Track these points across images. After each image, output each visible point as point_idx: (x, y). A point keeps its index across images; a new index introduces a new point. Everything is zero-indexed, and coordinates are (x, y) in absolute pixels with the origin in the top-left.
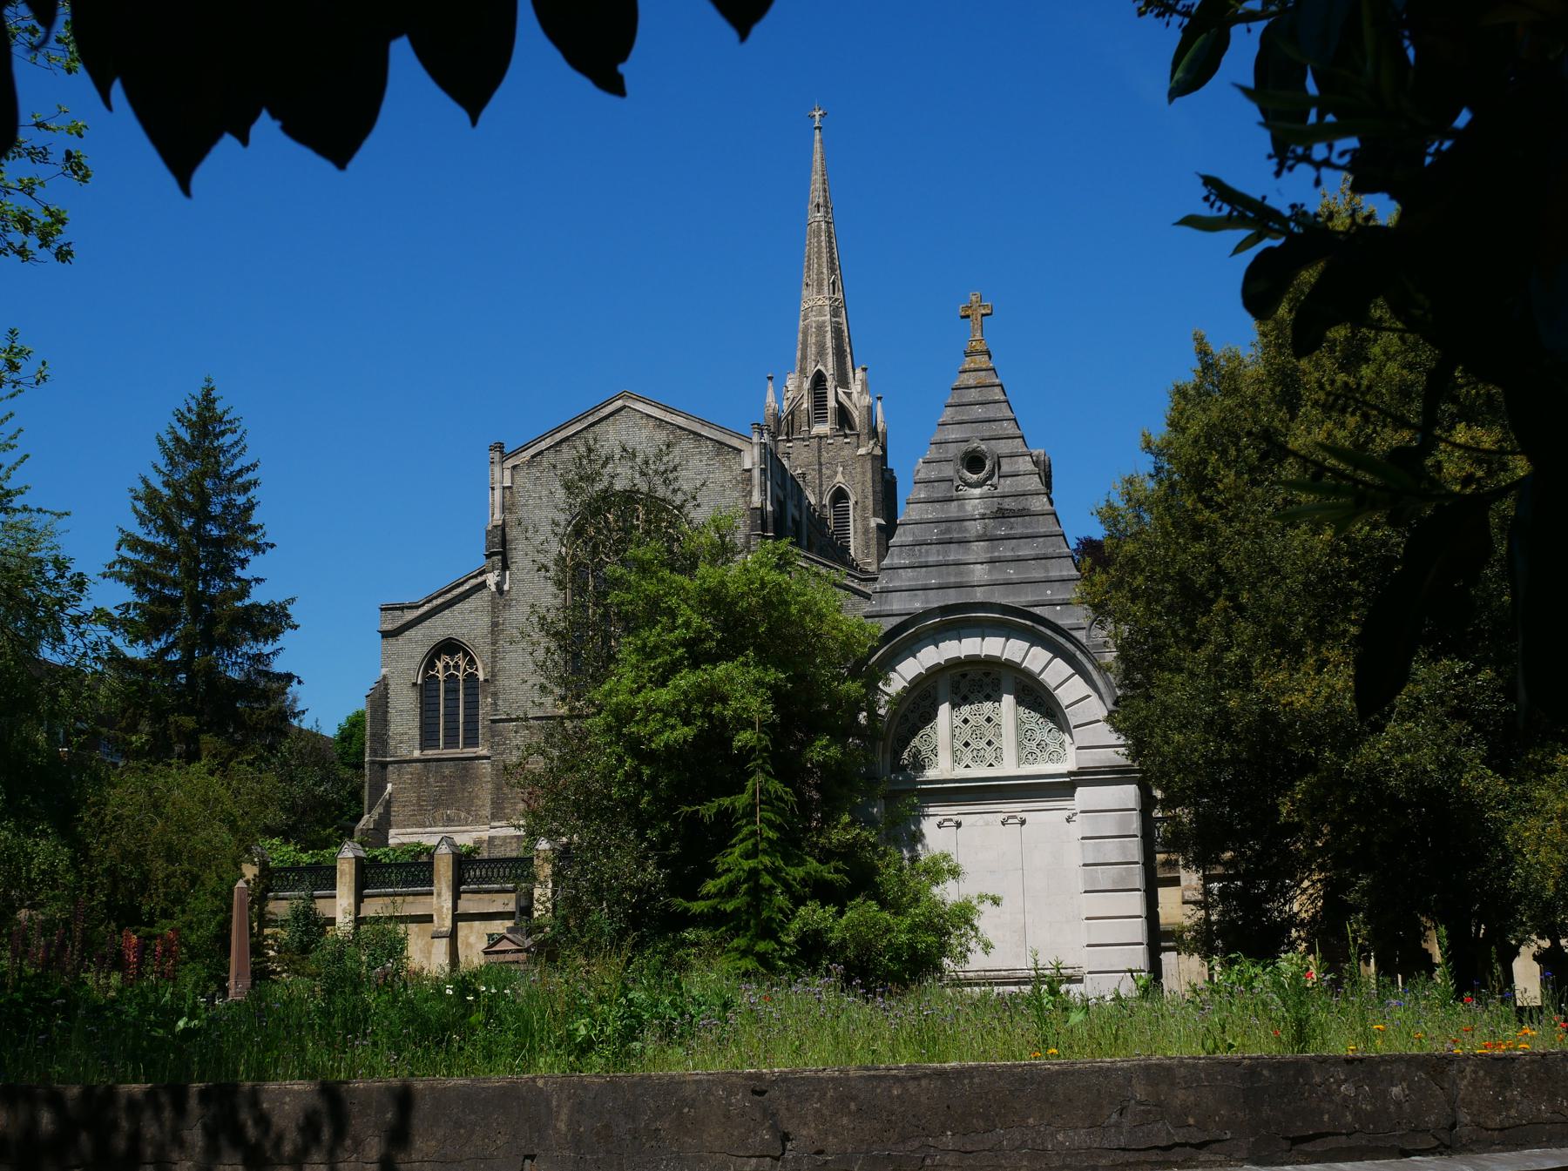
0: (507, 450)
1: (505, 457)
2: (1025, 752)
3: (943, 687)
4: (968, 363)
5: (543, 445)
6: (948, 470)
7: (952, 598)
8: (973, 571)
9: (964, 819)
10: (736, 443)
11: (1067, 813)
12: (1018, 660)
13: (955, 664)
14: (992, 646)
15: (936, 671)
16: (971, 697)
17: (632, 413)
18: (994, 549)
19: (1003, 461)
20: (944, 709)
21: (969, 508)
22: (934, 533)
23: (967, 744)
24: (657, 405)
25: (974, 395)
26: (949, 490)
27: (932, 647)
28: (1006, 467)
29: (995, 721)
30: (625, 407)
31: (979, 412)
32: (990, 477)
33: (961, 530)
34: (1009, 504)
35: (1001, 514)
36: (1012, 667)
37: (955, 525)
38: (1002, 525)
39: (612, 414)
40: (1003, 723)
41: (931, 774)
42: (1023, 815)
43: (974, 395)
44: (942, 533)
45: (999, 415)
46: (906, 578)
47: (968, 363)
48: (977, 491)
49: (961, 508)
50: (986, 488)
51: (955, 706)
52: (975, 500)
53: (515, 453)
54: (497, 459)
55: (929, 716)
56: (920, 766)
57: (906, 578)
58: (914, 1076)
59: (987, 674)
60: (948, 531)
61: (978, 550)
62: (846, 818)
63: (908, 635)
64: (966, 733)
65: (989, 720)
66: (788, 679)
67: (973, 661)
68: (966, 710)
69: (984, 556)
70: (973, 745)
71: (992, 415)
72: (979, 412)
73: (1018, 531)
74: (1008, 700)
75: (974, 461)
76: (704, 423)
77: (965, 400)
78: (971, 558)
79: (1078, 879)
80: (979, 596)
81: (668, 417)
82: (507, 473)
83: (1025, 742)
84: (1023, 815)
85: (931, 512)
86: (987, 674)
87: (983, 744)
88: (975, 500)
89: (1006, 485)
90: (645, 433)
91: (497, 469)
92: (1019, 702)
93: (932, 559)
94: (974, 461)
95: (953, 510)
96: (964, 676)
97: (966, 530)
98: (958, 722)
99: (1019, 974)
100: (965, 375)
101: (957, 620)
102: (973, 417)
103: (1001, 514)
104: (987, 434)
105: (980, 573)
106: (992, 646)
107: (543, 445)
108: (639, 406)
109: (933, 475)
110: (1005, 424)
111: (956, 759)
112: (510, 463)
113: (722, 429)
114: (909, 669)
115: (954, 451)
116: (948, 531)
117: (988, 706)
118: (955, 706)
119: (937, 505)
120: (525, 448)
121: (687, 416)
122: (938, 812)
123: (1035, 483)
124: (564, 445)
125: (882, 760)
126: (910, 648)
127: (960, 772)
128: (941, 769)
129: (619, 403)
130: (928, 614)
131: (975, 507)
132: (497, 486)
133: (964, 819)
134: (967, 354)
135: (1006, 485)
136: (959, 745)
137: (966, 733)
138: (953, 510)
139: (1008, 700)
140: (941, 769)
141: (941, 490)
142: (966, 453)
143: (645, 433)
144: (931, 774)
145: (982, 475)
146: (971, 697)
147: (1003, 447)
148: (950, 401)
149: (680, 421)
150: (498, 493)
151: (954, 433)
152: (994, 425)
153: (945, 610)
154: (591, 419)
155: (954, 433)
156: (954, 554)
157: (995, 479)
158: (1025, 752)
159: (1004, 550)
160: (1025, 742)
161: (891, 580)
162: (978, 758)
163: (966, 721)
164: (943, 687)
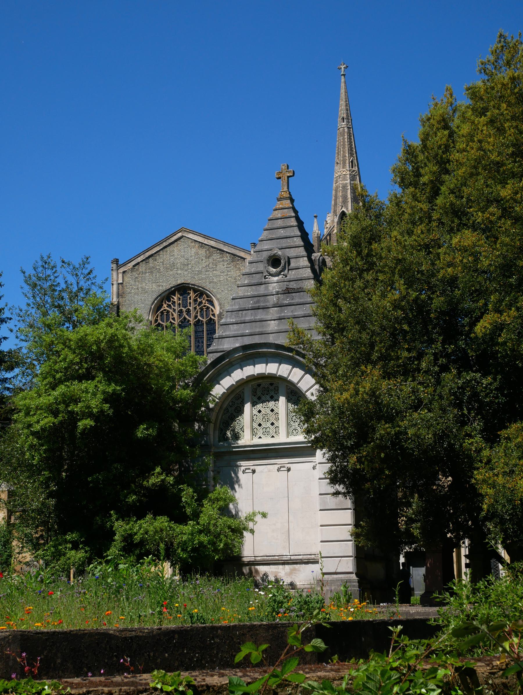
0: (120, 263)
1: (119, 267)
2: (292, 429)
3: (248, 392)
4: (279, 205)
5: (139, 259)
6: (261, 267)
7: (257, 340)
8: (269, 325)
9: (257, 468)
10: (242, 254)
11: (313, 464)
12: (285, 375)
13: (252, 379)
14: (272, 368)
15: (242, 384)
16: (263, 398)
17: (187, 240)
18: (282, 311)
19: (292, 261)
20: (247, 407)
21: (271, 288)
22: (250, 303)
23: (260, 425)
24: (200, 235)
25: (280, 223)
26: (261, 279)
27: (239, 370)
28: (293, 265)
29: (276, 411)
30: (182, 237)
31: (282, 232)
32: (283, 270)
33: (265, 301)
34: (293, 285)
35: (288, 291)
36: (282, 379)
37: (262, 299)
38: (287, 297)
39: (176, 241)
40: (280, 412)
41: (241, 442)
42: (289, 465)
43: (280, 223)
44: (255, 303)
45: (292, 234)
46: (233, 330)
47: (279, 205)
48: (276, 279)
49: (267, 288)
50: (281, 276)
51: (254, 404)
52: (275, 284)
53: (125, 264)
54: (115, 268)
55: (240, 411)
56: (236, 437)
57: (233, 330)
58: (18, 631)
59: (271, 384)
60: (258, 302)
61: (274, 312)
62: (158, 470)
63: (225, 363)
64: (259, 418)
65: (272, 410)
66: (123, 390)
67: (262, 377)
68: (259, 406)
69: (276, 316)
70: (264, 425)
71: (288, 234)
72: (282, 232)
73: (297, 300)
74: (282, 399)
75: (275, 261)
76: (225, 244)
77: (275, 226)
78: (269, 317)
79: (316, 502)
80: (271, 339)
81: (206, 242)
82: (120, 275)
83: (292, 423)
84: (289, 465)
85: (250, 291)
86: (271, 384)
87: (269, 424)
88: (275, 284)
89: (292, 275)
90: (194, 250)
91: (115, 273)
92: (289, 400)
93: (248, 318)
94: (275, 261)
95: (262, 290)
96: (259, 385)
97: (268, 301)
98: (255, 412)
99: (285, 558)
100: (276, 212)
101: (251, 353)
102: (278, 236)
103: (288, 291)
104: (284, 245)
105: (273, 326)
106: (272, 368)
107: (139, 259)
108: (191, 236)
109: (253, 270)
110: (295, 239)
111: (254, 433)
112: (121, 270)
113: (235, 247)
114: (227, 382)
115: (266, 255)
116: (258, 302)
117: (271, 404)
118: (254, 404)
119: (254, 287)
120: (130, 261)
121: (216, 240)
122: (244, 464)
123: (308, 273)
124: (151, 259)
125: (213, 436)
126: (227, 371)
127: (256, 441)
128: (246, 439)
129: (180, 235)
130: (236, 350)
131: (274, 288)
132: (115, 283)
133: (257, 468)
134: (279, 200)
135: (292, 275)
136: (255, 425)
137: (259, 418)
138: (262, 290)
139: (282, 399)
140: (246, 439)
141: (257, 279)
142: (270, 257)
143: (194, 250)
144: (241, 442)
145: (279, 269)
146: (263, 398)
147: (291, 253)
148: (266, 227)
149: (212, 243)
150: (115, 287)
151: (266, 246)
152: (289, 240)
153: (245, 348)
154: (165, 244)
155: (266, 246)
156: (260, 315)
157: (286, 271)
158: (292, 429)
159: (287, 312)
160: (292, 423)
161: (225, 331)
162: (266, 433)
163: (260, 411)
164: (248, 392)
